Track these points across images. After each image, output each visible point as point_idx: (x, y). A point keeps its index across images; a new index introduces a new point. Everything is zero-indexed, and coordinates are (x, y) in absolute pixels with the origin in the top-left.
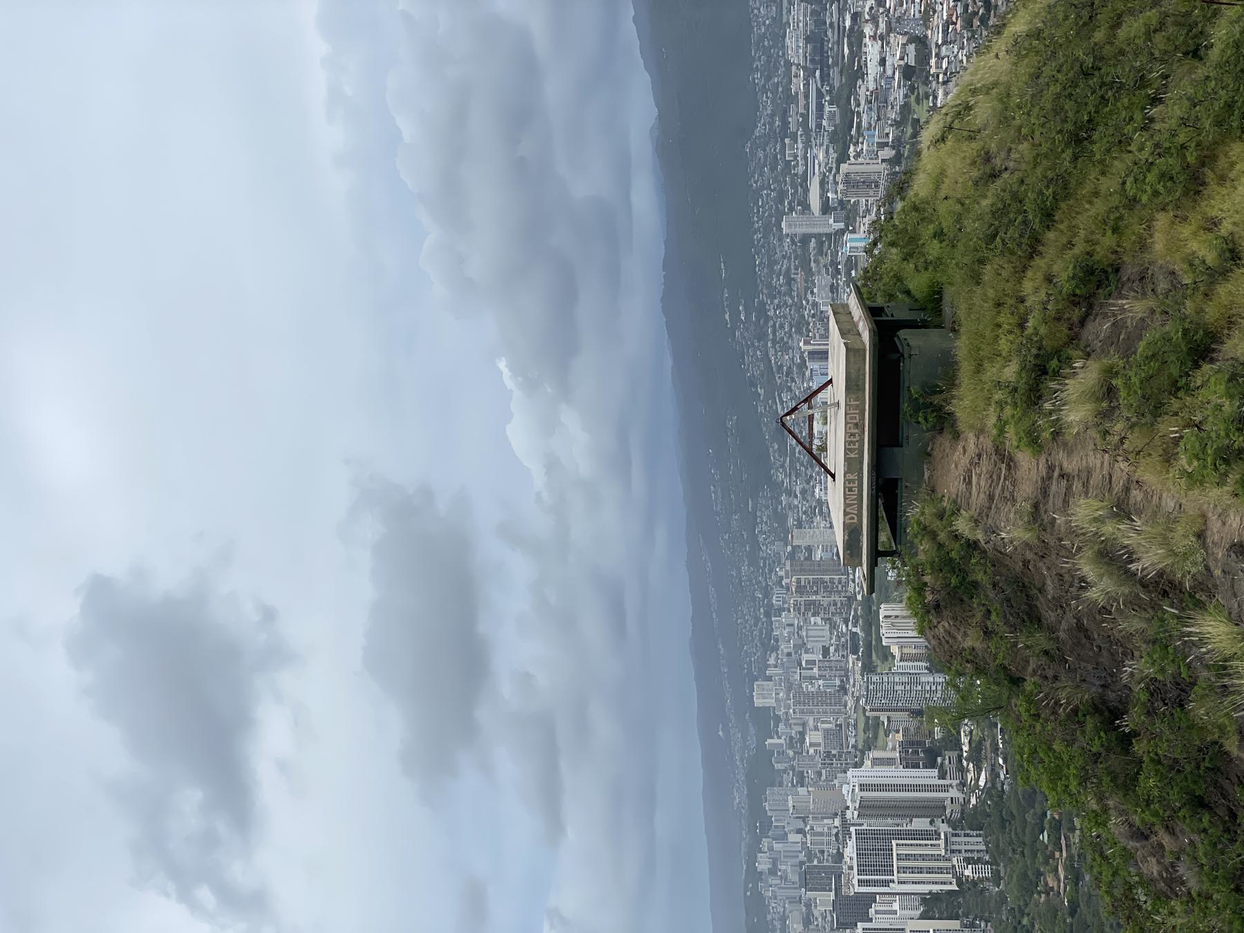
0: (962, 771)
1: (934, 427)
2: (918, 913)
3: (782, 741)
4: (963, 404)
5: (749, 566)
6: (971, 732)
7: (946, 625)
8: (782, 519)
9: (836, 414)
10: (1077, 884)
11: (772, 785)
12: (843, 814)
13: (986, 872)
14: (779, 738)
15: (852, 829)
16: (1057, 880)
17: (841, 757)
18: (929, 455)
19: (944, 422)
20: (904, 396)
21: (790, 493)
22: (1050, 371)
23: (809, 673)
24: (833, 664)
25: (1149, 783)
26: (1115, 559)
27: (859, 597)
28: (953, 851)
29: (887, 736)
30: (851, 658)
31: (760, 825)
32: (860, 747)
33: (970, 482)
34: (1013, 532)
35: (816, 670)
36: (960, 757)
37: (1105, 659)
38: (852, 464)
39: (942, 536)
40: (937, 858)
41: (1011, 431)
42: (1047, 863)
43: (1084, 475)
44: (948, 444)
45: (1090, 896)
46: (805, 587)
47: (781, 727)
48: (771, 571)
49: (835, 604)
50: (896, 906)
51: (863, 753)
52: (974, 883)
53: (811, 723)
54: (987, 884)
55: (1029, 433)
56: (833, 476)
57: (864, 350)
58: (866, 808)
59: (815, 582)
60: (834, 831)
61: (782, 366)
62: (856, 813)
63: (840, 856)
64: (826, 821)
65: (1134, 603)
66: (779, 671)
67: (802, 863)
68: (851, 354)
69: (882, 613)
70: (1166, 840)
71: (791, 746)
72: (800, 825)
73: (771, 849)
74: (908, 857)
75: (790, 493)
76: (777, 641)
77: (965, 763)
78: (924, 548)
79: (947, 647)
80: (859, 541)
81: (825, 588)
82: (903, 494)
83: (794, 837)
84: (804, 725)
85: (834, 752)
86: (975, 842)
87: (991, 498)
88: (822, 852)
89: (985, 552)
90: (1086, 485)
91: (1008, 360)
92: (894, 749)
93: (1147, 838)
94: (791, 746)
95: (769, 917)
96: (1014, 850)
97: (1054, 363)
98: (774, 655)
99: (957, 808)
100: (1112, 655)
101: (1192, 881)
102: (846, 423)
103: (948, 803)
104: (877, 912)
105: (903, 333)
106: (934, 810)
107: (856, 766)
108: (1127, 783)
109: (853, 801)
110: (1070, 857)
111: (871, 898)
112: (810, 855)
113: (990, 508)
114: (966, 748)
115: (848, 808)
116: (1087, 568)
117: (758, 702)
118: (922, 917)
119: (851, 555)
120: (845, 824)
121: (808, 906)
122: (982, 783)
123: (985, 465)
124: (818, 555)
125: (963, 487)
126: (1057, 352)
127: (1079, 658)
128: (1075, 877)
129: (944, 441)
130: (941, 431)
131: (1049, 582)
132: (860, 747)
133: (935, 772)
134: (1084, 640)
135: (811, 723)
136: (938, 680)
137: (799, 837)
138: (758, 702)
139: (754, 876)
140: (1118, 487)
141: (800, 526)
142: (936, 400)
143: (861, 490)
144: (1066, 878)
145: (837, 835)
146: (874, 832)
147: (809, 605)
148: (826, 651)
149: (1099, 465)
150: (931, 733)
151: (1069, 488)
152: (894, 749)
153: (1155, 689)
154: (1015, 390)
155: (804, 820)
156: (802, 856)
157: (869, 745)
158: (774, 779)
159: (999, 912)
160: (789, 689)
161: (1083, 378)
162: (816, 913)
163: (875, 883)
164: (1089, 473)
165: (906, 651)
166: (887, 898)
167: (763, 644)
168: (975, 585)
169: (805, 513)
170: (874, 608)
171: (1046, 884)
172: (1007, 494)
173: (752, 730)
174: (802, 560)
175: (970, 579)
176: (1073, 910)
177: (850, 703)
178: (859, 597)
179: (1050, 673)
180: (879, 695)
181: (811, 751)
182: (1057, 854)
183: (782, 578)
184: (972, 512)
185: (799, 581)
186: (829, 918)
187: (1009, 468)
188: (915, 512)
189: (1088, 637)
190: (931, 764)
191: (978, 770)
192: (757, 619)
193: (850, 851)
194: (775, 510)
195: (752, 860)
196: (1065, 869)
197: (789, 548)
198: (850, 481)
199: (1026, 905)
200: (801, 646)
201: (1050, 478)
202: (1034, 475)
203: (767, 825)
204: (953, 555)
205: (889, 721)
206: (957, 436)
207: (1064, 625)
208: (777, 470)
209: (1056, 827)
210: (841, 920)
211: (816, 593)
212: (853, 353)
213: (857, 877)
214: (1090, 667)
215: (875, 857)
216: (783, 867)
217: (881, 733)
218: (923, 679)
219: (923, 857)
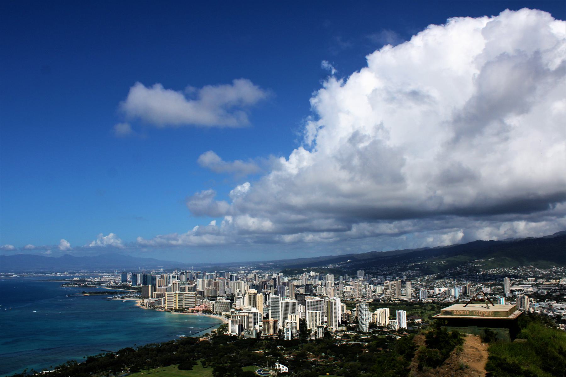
11: (335, 276)
13: (313, 337)
21: (422, 281)
30: (372, 300)
50: (302, 311)
51: (345, 303)
63: (315, 295)
69: (386, 309)
72: (323, 284)
75: (422, 281)
86: (321, 334)
106: (329, 323)
111: (304, 304)
112: (315, 287)
114: (347, 333)
117: (358, 272)
118: (300, 319)
124: (403, 289)
141: (411, 284)
148: (374, 292)
156: (315, 285)
192: (383, 271)
193: (317, 299)
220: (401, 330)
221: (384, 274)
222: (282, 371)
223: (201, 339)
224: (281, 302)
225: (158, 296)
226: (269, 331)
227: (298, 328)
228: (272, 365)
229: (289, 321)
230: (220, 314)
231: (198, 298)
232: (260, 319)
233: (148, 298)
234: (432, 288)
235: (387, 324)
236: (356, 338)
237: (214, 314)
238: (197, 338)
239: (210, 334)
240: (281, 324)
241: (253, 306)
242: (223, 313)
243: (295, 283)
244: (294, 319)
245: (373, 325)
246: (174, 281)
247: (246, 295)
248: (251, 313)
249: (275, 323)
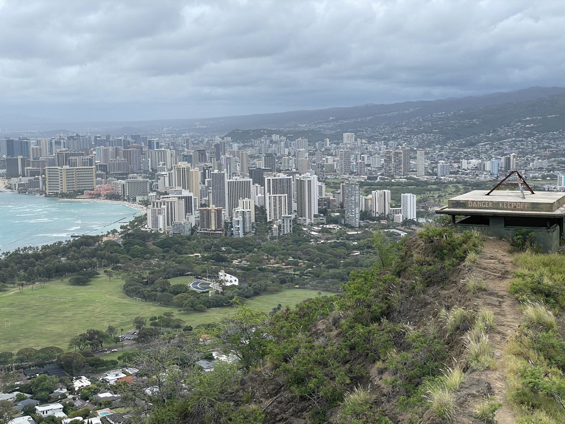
0: (318, 225)
1: (514, 242)
2: (257, 205)
3: (328, 146)
4: (527, 256)
5: (407, 130)
6: (334, 229)
7: (422, 245)
8: (429, 146)
9: (518, 196)
10: (272, 272)
11: (309, 141)
12: (297, 173)
13: (275, 234)
14: (330, 145)
15: (291, 177)
16: (273, 264)
17: (322, 171)
18: (501, 239)
19: (518, 247)
20: (529, 229)
21: (441, 149)
22: (548, 298)
23: (359, 158)
24: (363, 169)
25: (360, 329)
26: (464, 326)
27: (393, 181)
28: (283, 220)
29: (332, 192)
30: (366, 177)
31: (292, 136)
32: (326, 180)
33: (491, 259)
34: (472, 281)
35: (360, 161)
36: (323, 224)
37: (412, 313)
38: (496, 205)
39: (465, 246)
40: (280, 214)
41: (518, 281)
42: (280, 259)
43: (502, 313)
44: (506, 248)
45: (267, 277)
46: (398, 156)
47: (335, 145)
48: (405, 140)
49: (390, 170)
50: (259, 195)
51: (324, 182)
52: (270, 229)
53: (336, 159)
54: (270, 234)
55: (521, 290)
56: (488, 194)
57: (552, 211)
58: (300, 183)
59: (400, 161)
60: (290, 169)
61: (503, 145)
62: (298, 179)
63: (279, 171)
64: (294, 165)
65: (441, 331)
66: (359, 144)
67: (276, 154)
68: (550, 205)
69: (386, 191)
70: (335, 332)
71: (326, 150)
72: (292, 154)
73: (281, 141)
74: (280, 201)
76: (373, 143)
77: (321, 226)
78: (458, 236)
79: (412, 244)
80: (460, 207)
81: (397, 165)
82: (484, 227)
83: (287, 151)
84: (336, 155)
85: (324, 169)
86: (287, 230)
87: (485, 269)
88: (281, 163)
89: (459, 264)
90: (498, 314)
91: (551, 279)
92: (326, 195)
93: (334, 325)
94: (326, 150)
95: (252, 140)
96: (285, 246)
97: (552, 300)
98: (366, 142)
99: (302, 222)
100: (415, 317)
101: (319, 342)
102: (516, 203)
103: (304, 218)
104: (257, 187)
105: (558, 227)
106: (301, 212)
107: (318, 178)
108: (357, 319)
109: (303, 177)
110: (283, 269)
111: (263, 185)
112: (279, 158)
113: (480, 268)
114: (328, 226)
115: (300, 175)
116: (458, 312)
117: (345, 135)
118: (255, 206)
119: (453, 204)
120: (293, 174)
121: (258, 157)
122: (313, 233)
123: (499, 266)
124: (413, 162)
125: (489, 255)
126: (557, 302)
127: (412, 302)
128: (275, 271)
129: (508, 246)
130: (512, 245)
131: (446, 292)
132: (326, 180)
133: (317, 213)
134: (420, 305)
135: (336, 159)
136: (357, 215)
137: (287, 153)
138: (345, 135)
139: (270, 133)
140: (499, 329)
141: (426, 153)
142: (528, 243)
143: (484, 208)
144: (274, 267)
145: (288, 170)
146: (290, 186)
147: (390, 158)
148: (369, 165)
149: (508, 320)
150: (333, 212)
151: (495, 306)
152: (326, 195)
153: (401, 335)
154: (539, 283)
155: (294, 155)
156: (279, 154)
157: (327, 184)
158: (311, 142)
159: (259, 239)
160: (352, 149)
161: (547, 315)
162: (255, 161)
163: (269, 187)
164: (504, 315)
165: (370, 201)
166: (263, 191)
167: (371, 137)
168: (443, 259)
169: (432, 156)
170: (388, 187)
171: (271, 259)
172: (488, 276)
173: (333, 132)
174: (410, 155)
175: (445, 257)
176: (261, 270)
177: (346, 176)
178: (393, 181)
179: (404, 289)
180: (350, 189)
181: (324, 159)
182: (284, 264)
183: (402, 145)
184: (478, 260)
185: (400, 153)
186: (253, 166)
187: (499, 277)
188: (475, 232)
189: (422, 307)
190: (320, 211)
191: (319, 232)
192: (382, 134)
193: (282, 176)
194: (433, 142)
195: (276, 132)
196: (278, 267)
197: (415, 149)
198: (488, 204)
199: (263, 250)
200: (371, 154)
201: (498, 296)
202: (497, 289)
203: (292, 139)
204: (457, 251)
205: (338, 193)
206: (511, 252)
207: (427, 297)
208: (452, 143)
209: (296, 264)
210: (253, 172)
211: (395, 161)
212: (550, 206)
213: (271, 179)
214: (408, 307)
215: (280, 187)
216: (274, 146)
217: (333, 190)
218: (357, 209)
219: (280, 207)
220: (407, 223)
221: (385, 139)
222: (228, 284)
223: (105, 239)
224: (227, 180)
225: (33, 174)
226: (209, 225)
227: (253, 220)
228: (214, 276)
229: (240, 209)
230: (134, 200)
231: (98, 176)
232: (195, 206)
233: (17, 176)
234: (457, 160)
235: (387, 213)
236: (340, 234)
237: (124, 200)
238: (98, 236)
239: (119, 230)
240: (227, 213)
241: (184, 188)
242: (139, 198)
243: (249, 151)
244: (246, 207)
245: (365, 215)
246: (58, 150)
248: (182, 198)
249: (219, 212)
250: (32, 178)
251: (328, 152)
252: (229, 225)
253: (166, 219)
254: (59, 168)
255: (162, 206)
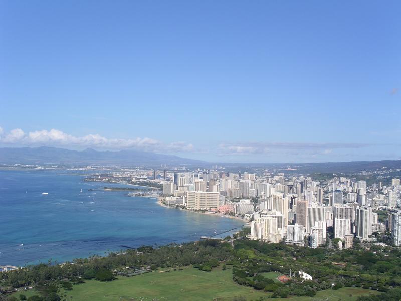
11: (367, 183)
47: (385, 187)
138: (394, 180)
227: (325, 236)
247: (270, 198)
250: (179, 198)
251: (381, 192)
252: (309, 240)
253: (368, 215)
254: (196, 192)
255: (262, 222)
